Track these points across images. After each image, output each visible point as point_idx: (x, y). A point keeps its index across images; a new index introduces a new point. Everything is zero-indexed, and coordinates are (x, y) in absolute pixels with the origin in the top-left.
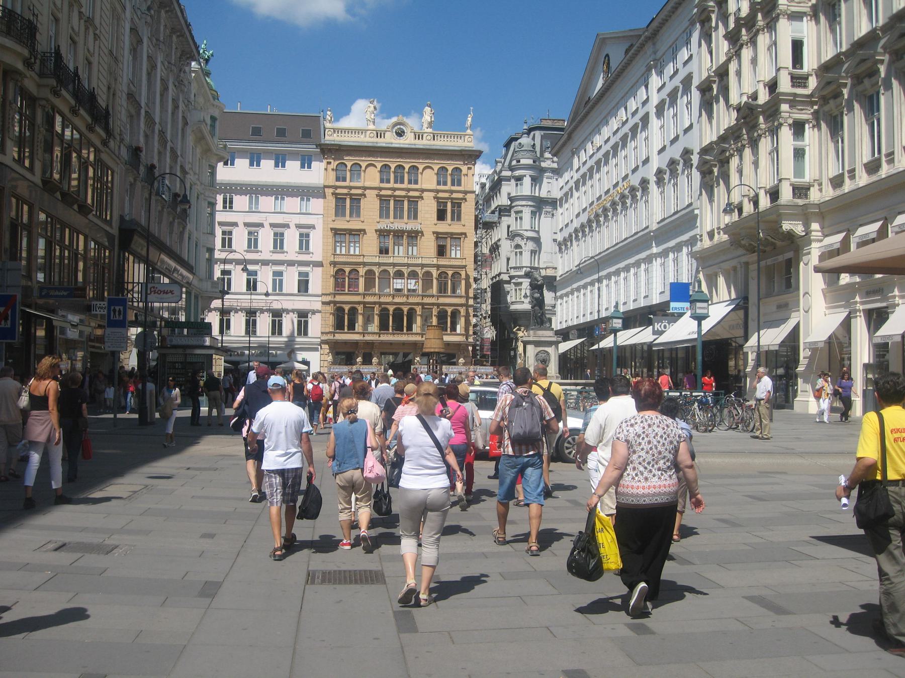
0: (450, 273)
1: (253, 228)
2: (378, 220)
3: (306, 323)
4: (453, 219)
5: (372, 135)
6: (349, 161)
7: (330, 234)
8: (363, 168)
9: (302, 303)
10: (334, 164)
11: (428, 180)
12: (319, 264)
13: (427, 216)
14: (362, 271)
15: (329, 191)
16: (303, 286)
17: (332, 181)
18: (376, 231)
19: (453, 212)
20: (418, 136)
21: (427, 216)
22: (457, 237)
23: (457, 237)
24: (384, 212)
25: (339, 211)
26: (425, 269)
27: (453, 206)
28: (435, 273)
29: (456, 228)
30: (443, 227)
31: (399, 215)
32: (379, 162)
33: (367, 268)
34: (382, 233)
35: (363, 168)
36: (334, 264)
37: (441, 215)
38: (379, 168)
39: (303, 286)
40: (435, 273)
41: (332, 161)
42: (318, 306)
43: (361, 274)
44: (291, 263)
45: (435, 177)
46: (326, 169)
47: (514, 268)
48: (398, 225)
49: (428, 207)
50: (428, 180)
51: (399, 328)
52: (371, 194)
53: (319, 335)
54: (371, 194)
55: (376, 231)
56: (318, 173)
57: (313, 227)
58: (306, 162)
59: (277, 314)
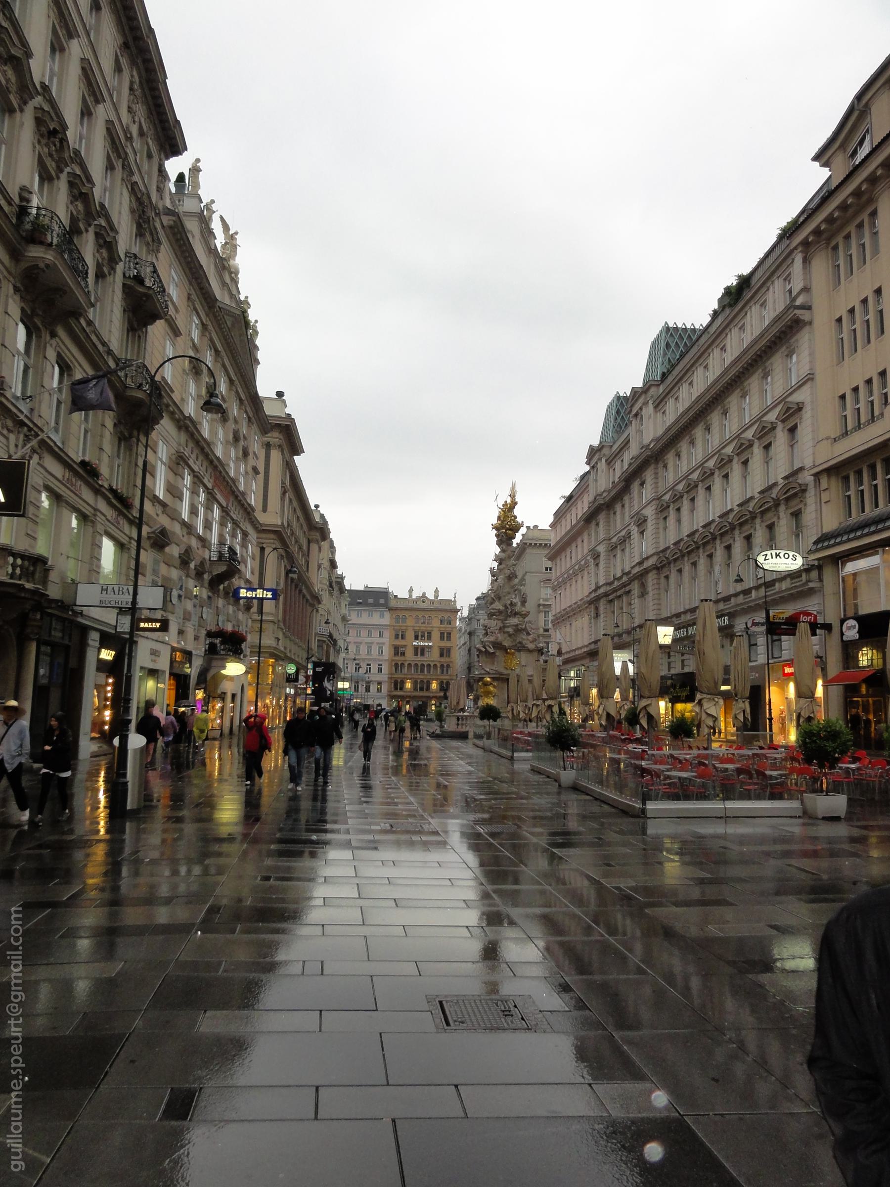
1: (358, 645)
6: (401, 614)
9: (379, 678)
11: (436, 623)
12: (386, 660)
16: (380, 670)
20: (432, 602)
25: (397, 637)
28: (439, 665)
32: (414, 614)
39: (380, 670)
40: (439, 665)
42: (386, 679)
44: (374, 660)
49: (436, 635)
51: (422, 689)
52: (410, 629)
54: (410, 629)
56: (386, 619)
57: (384, 644)
58: (382, 615)
59: (368, 683)
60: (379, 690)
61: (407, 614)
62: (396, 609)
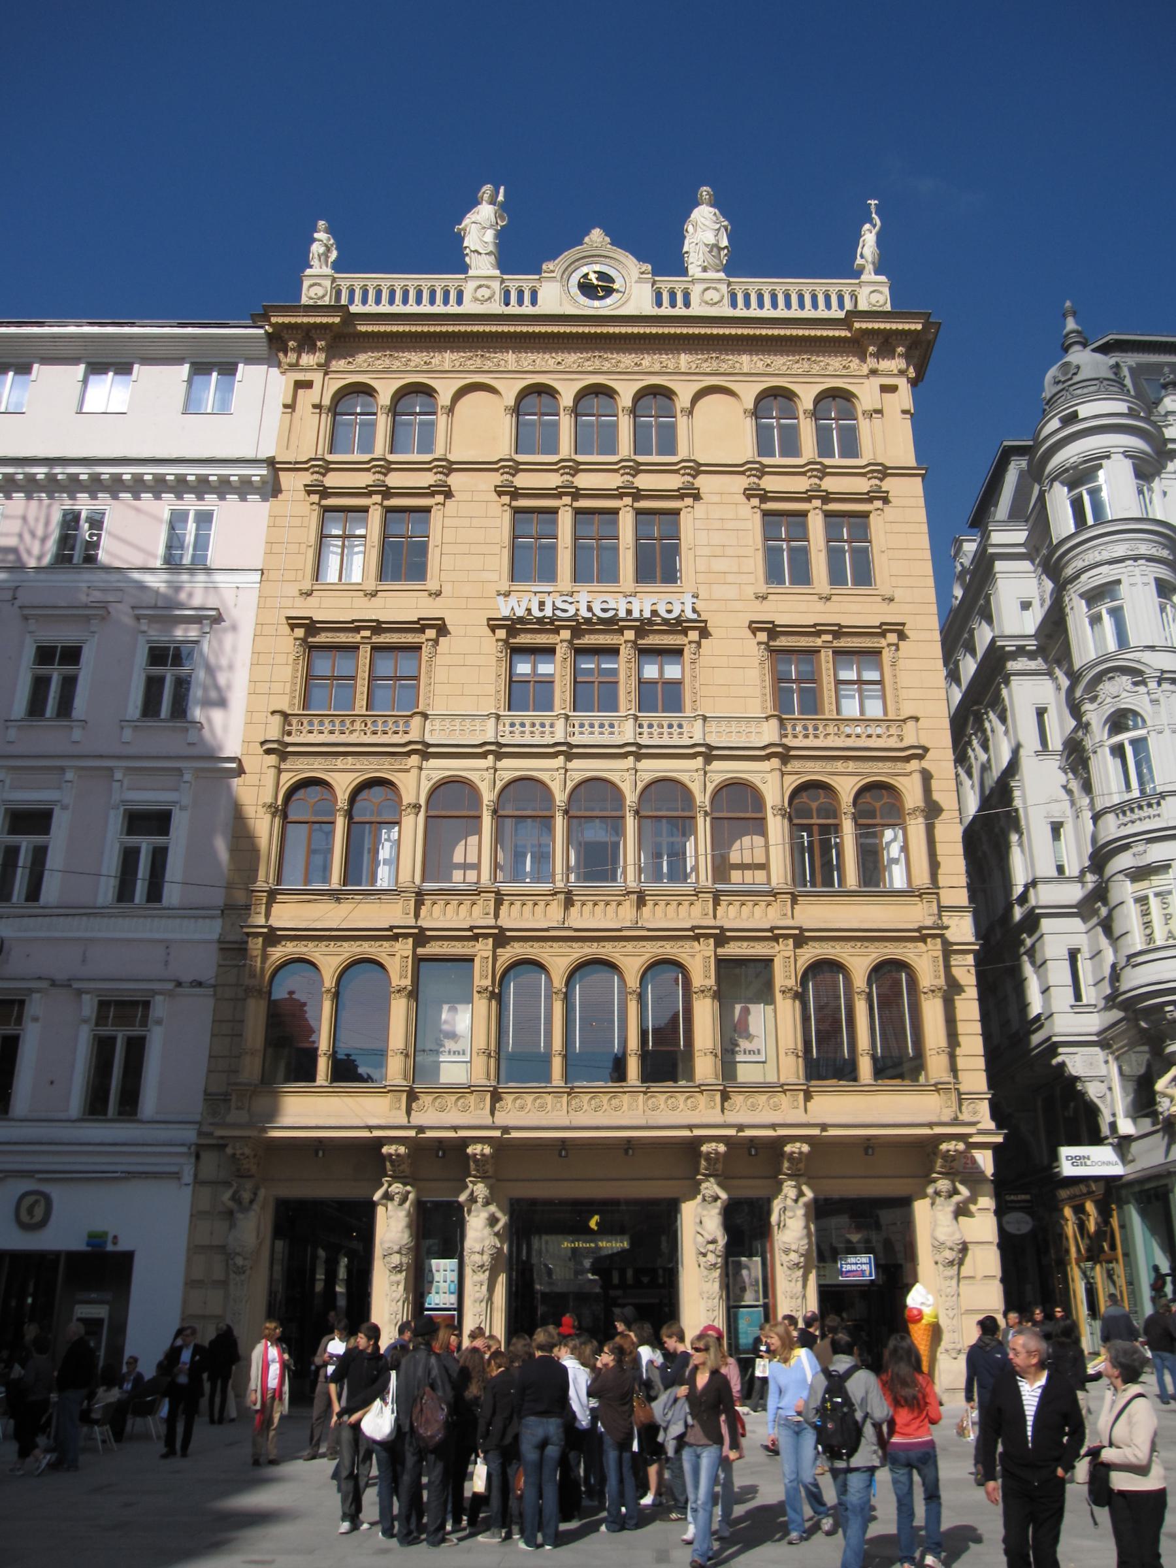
0: (846, 787)
2: (505, 585)
3: (137, 1047)
4: (836, 577)
5: (486, 292)
6: (386, 374)
7: (287, 644)
8: (444, 398)
10: (325, 388)
13: (720, 565)
14: (414, 783)
15: (293, 483)
17: (309, 436)
18: (493, 625)
19: (834, 556)
21: (720, 565)
22: (863, 649)
23: (863, 649)
24: (528, 560)
26: (723, 770)
27: (832, 536)
29: (855, 609)
30: (794, 608)
31: (594, 565)
33: (438, 769)
34: (519, 638)
35: (444, 398)
36: (280, 751)
37: (785, 564)
38: (510, 399)
41: (317, 377)
43: (408, 798)
45: (749, 424)
46: (290, 407)
47: (1121, 809)
48: (588, 600)
50: (718, 430)
52: (476, 495)
53: (196, 1107)
54: (476, 495)
55: (493, 625)
60: (114, 1084)
61: (444, 371)
62: (343, 335)
